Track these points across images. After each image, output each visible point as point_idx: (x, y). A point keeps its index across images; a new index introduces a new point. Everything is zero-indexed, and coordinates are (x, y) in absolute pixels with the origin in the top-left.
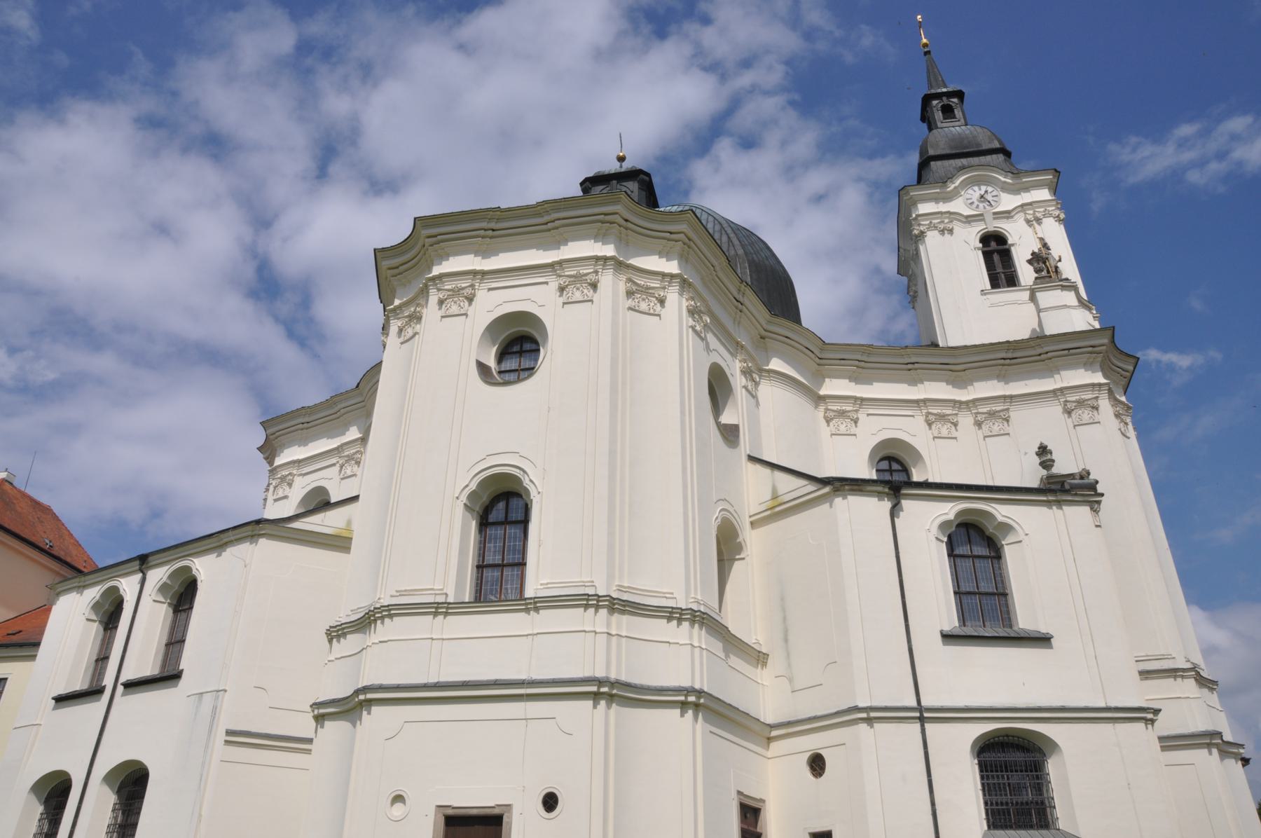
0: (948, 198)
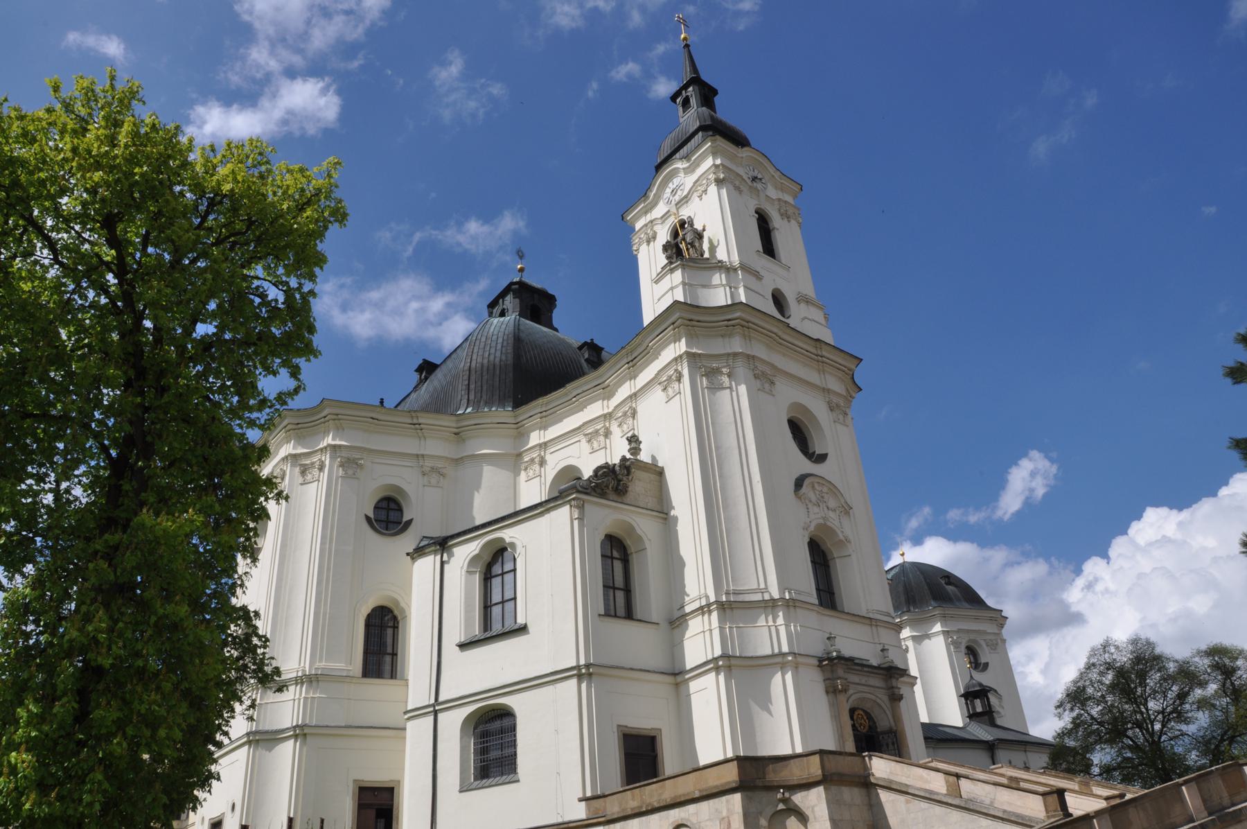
0: (654, 204)
